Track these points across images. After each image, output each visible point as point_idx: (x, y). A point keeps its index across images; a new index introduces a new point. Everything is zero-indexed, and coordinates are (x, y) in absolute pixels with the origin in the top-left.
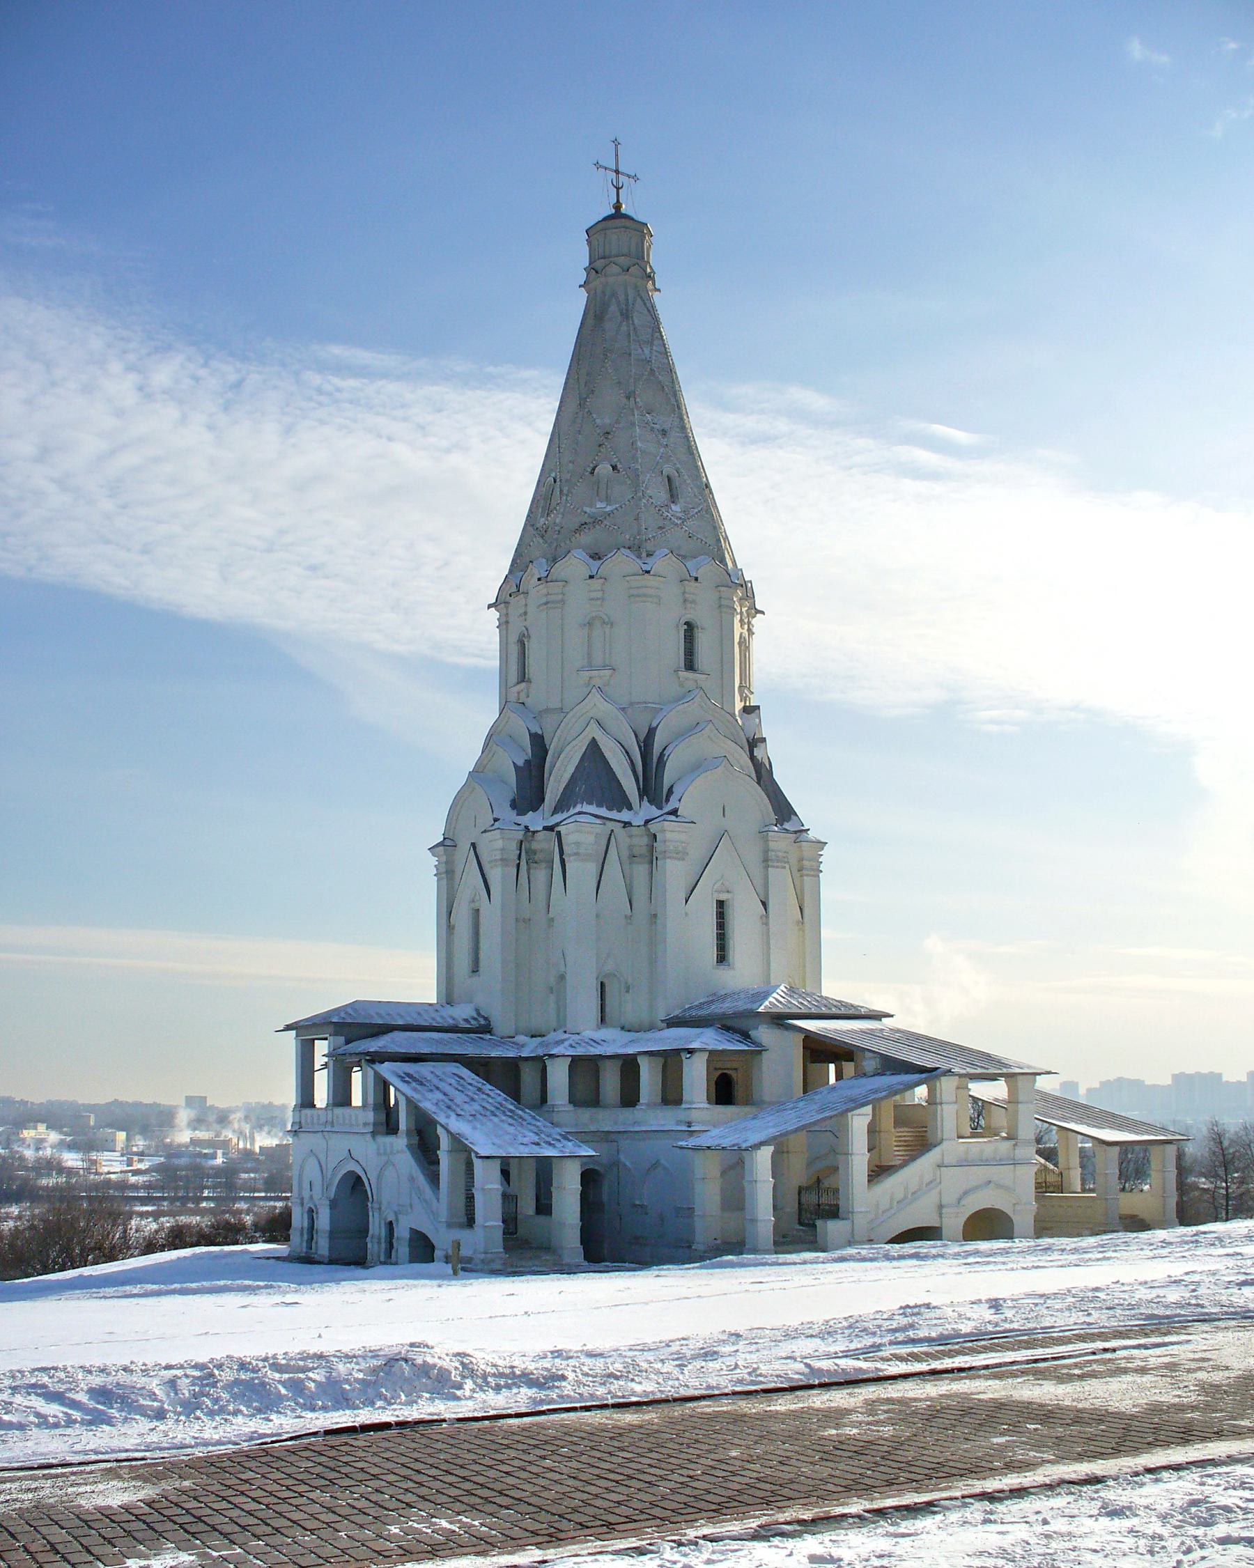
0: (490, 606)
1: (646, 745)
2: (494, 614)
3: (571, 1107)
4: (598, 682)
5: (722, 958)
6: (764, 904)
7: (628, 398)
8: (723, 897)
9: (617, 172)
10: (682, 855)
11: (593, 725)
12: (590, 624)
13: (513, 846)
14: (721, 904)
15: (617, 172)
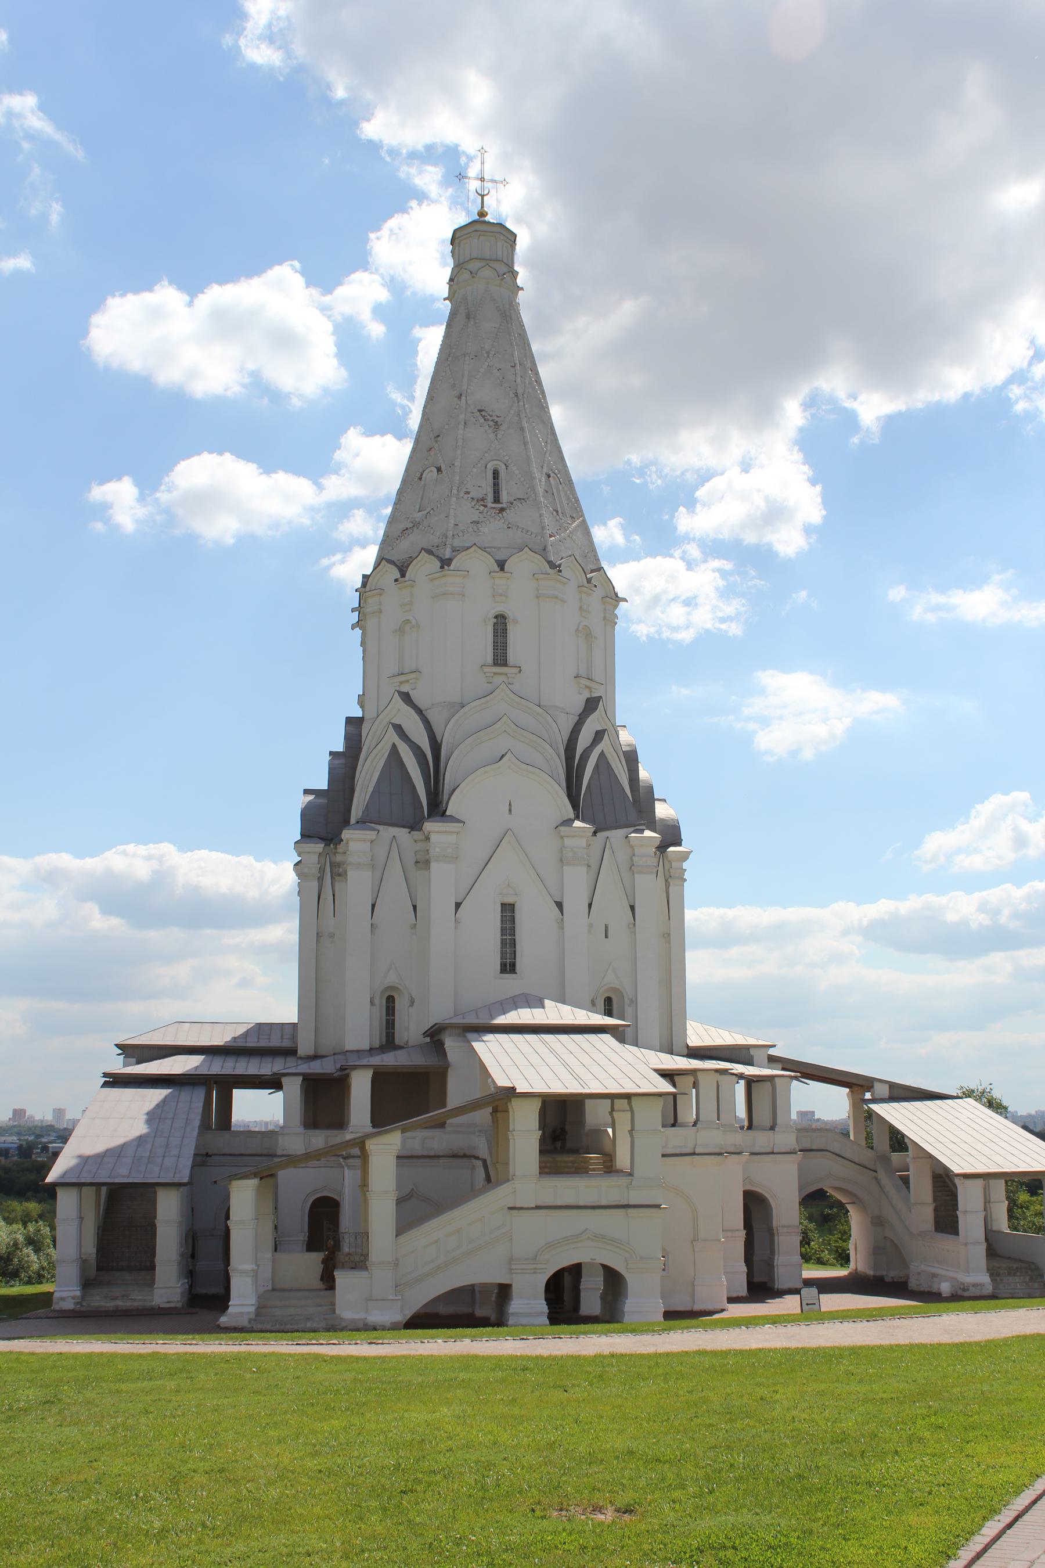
0: (353, 627)
1: (436, 746)
2: (358, 631)
3: (301, 1130)
4: (404, 689)
5: (508, 967)
6: (560, 905)
7: (460, 397)
8: (509, 900)
9: (482, 179)
10: (454, 859)
11: (391, 730)
12: (401, 631)
13: (315, 858)
14: (508, 910)
15: (482, 179)
